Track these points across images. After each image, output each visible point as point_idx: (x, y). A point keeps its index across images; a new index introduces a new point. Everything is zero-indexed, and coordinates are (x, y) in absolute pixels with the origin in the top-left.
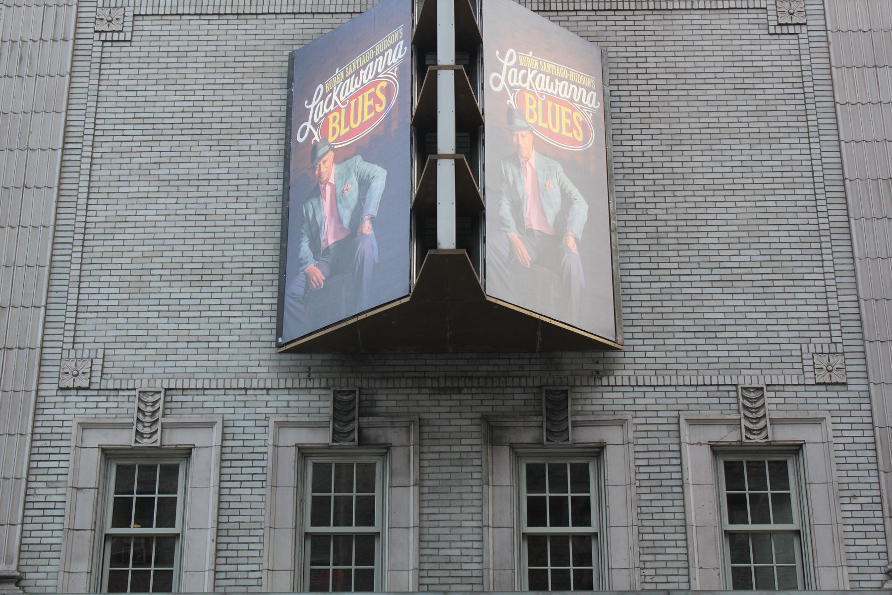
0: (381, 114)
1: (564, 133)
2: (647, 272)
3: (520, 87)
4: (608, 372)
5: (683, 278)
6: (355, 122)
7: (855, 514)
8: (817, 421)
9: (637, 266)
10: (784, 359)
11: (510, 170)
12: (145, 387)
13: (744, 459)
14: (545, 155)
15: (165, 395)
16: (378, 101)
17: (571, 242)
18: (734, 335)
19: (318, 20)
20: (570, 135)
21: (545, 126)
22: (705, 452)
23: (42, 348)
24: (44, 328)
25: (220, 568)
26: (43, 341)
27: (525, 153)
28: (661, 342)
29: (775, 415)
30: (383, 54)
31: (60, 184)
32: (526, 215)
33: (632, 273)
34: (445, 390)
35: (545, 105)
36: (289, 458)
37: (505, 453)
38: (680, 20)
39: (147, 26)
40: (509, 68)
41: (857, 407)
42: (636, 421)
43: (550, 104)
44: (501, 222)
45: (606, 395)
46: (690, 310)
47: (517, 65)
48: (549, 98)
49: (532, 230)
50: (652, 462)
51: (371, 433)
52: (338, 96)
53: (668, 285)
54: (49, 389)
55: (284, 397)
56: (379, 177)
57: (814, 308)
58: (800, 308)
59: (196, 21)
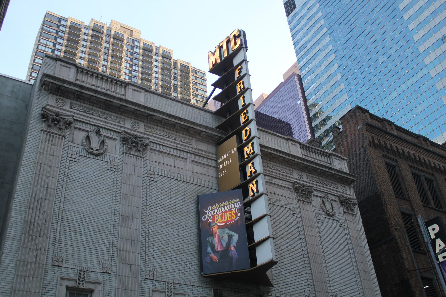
0: (234, 219)
6: (225, 219)
12: (168, 281)
16: (232, 215)
19: (200, 188)
30: (233, 204)
39: (161, 179)
52: (217, 211)
56: (236, 237)
59: (172, 181)
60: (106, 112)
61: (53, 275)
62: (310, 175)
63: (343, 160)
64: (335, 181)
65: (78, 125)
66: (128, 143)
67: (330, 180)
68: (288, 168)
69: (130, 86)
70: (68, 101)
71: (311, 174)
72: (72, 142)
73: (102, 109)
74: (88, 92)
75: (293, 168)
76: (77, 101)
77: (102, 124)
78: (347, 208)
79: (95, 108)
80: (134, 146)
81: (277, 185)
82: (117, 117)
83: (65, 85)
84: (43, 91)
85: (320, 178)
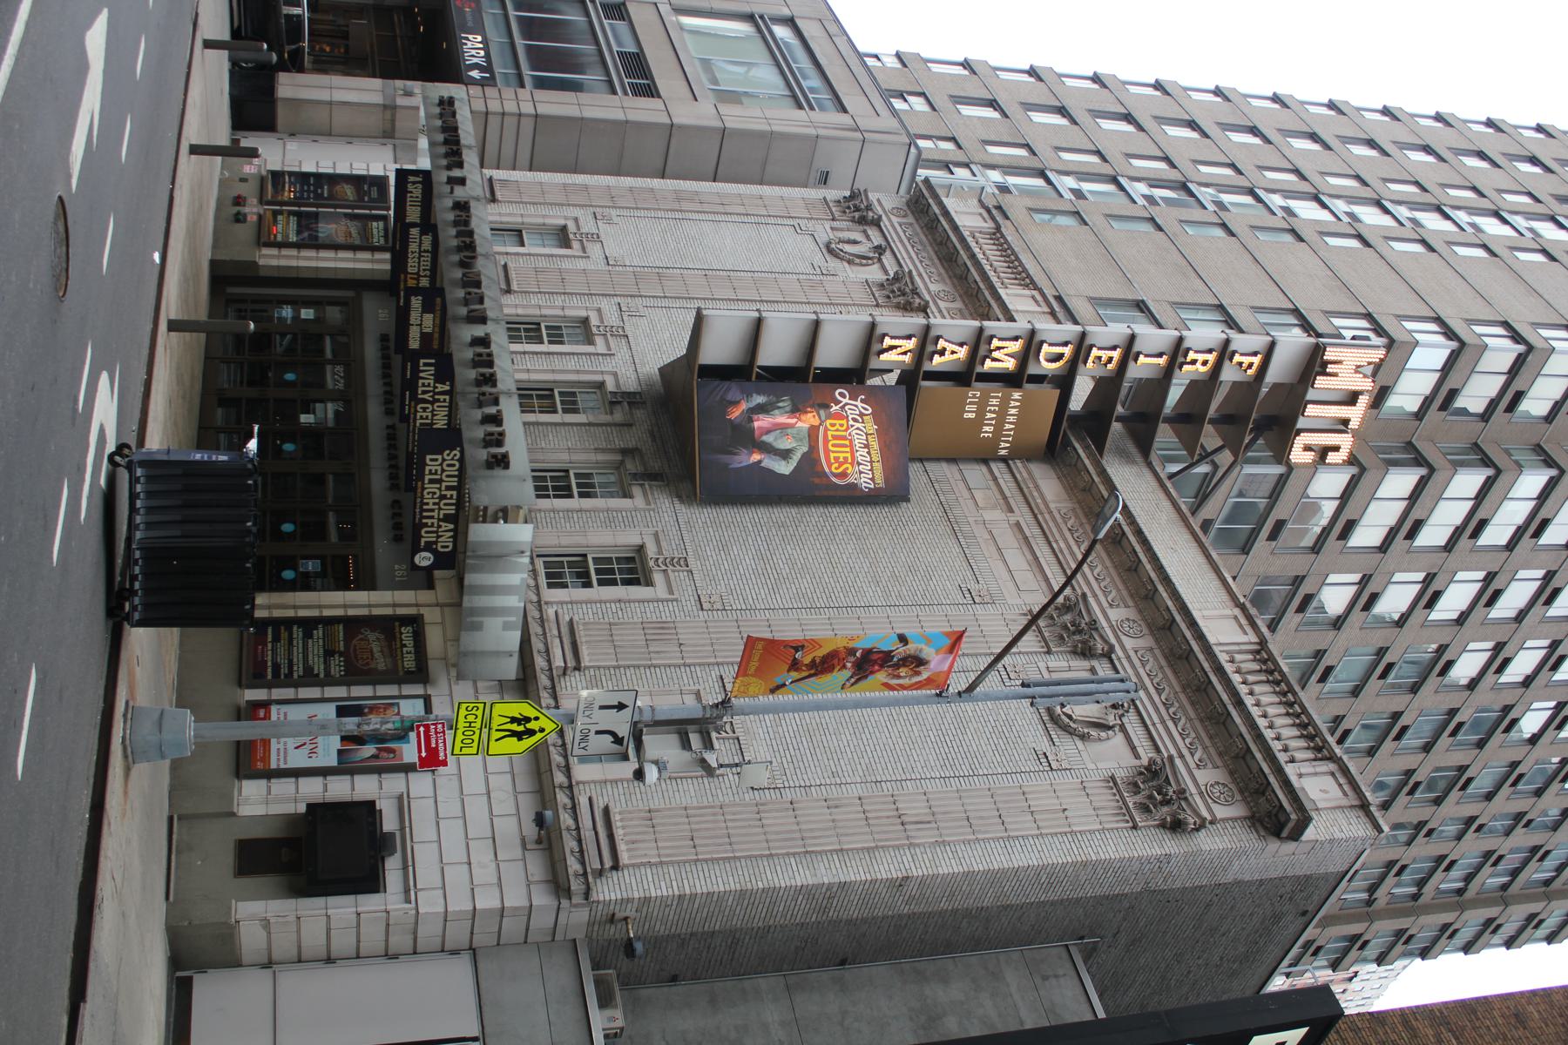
4: (682, 501)
8: (671, 592)
11: (785, 403)
13: (638, 565)
17: (756, 457)
22: (637, 541)
35: (844, 438)
36: (598, 378)
37: (619, 457)
38: (952, 542)
44: (749, 395)
47: (861, 415)
51: (618, 407)
61: (577, 212)
62: (1163, 663)
63: (1364, 819)
64: (1220, 754)
67: (1211, 738)
68: (1125, 593)
69: (1035, 293)
70: (911, 219)
71: (1171, 666)
75: (1137, 606)
78: (1135, 785)
81: (1036, 558)
85: (1182, 697)
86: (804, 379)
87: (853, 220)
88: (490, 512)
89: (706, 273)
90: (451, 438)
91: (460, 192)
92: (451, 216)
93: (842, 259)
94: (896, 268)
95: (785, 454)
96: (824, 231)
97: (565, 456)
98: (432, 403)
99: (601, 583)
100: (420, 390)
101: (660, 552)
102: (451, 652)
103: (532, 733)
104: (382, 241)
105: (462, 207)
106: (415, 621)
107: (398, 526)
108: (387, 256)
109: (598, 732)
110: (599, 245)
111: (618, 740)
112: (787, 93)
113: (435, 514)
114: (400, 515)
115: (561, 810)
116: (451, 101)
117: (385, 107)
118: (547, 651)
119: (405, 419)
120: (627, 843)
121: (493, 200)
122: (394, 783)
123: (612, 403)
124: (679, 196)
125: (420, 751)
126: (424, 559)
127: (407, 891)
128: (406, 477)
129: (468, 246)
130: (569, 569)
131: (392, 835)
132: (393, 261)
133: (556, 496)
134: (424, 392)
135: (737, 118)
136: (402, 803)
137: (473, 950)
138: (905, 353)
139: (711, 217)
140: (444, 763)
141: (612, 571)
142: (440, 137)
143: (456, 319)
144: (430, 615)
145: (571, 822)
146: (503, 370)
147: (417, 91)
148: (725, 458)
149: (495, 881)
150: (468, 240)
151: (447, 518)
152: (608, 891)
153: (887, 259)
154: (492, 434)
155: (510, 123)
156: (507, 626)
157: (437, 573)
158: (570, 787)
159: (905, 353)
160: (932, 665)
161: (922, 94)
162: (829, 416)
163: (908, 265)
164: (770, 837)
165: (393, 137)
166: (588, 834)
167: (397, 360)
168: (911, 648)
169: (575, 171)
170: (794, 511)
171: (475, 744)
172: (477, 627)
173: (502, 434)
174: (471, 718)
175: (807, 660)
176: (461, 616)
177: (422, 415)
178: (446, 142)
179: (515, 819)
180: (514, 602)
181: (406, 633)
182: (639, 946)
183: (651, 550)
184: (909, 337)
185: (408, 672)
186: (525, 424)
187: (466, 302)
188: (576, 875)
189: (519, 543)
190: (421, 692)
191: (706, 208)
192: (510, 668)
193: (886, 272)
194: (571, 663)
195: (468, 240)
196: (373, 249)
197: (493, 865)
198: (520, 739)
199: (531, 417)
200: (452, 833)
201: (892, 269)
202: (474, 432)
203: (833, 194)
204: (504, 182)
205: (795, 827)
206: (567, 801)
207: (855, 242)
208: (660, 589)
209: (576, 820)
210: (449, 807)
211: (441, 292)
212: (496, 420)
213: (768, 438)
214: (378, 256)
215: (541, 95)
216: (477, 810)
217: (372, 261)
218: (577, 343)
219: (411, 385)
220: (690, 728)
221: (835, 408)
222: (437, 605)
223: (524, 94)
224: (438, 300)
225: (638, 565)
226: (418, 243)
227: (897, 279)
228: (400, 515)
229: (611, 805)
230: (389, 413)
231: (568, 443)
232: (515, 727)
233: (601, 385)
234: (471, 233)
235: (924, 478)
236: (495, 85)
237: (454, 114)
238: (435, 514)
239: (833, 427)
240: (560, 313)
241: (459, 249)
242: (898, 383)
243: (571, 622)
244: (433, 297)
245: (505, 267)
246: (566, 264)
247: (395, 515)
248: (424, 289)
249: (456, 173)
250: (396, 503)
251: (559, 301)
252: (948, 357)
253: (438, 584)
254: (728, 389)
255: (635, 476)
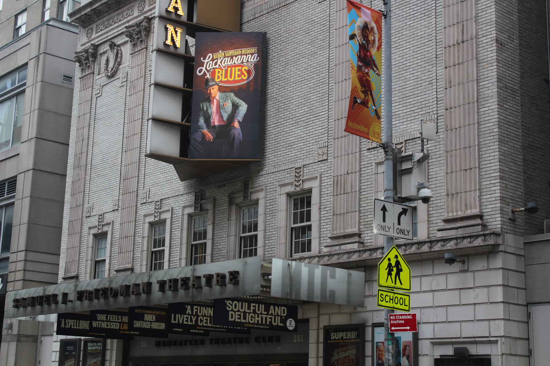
1: (237, 78)
2: (274, 125)
3: (213, 68)
4: (261, 170)
5: (285, 125)
7: (325, 215)
8: (316, 178)
9: (272, 123)
10: (311, 153)
11: (205, 106)
14: (225, 92)
15: (161, 201)
17: (236, 124)
18: (296, 146)
20: (240, 78)
21: (226, 79)
22: (284, 198)
23: (137, 191)
24: (138, 183)
25: (171, 260)
26: (138, 188)
27: (213, 95)
28: (276, 154)
29: (303, 178)
31: (141, 131)
32: (212, 121)
33: (271, 126)
34: (221, 186)
35: (226, 71)
36: (186, 217)
40: (207, 63)
41: (329, 169)
42: (268, 188)
43: (229, 69)
44: (199, 128)
45: (261, 179)
46: (285, 138)
47: (213, 60)
48: (228, 67)
49: (215, 126)
50: (271, 204)
51: (204, 206)
53: (280, 129)
54: (139, 204)
55: (186, 196)
57: (321, 128)
58: (317, 129)
60: (120, 11)
65: (102, 50)
66: (134, 39)
70: (94, 26)
72: (99, 75)
73: (117, 10)
74: (96, 5)
76: (99, 19)
77: (115, 32)
79: (112, 15)
80: (138, 38)
82: (128, 9)
83: (83, 13)
84: (82, 30)
86: (191, 93)
87: (94, 62)
88: (264, 284)
89: (124, 151)
90: (219, 306)
91: (71, 297)
92: (86, 302)
93: (118, 69)
94: (125, 36)
95: (235, 107)
96: (100, 79)
97: (232, 239)
98: (198, 316)
99: (309, 220)
100: (190, 323)
101: (291, 184)
102: (347, 310)
103: (398, 263)
104: (99, 344)
105: (81, 295)
106: (328, 331)
107: (271, 339)
108: (109, 341)
109: (399, 224)
110: (106, 215)
111: (404, 212)
112: (15, 98)
113: (264, 316)
114: (264, 338)
115: (445, 248)
116: (16, 301)
117: (18, 341)
118: (348, 253)
119: (206, 333)
120: (466, 209)
121: (76, 277)
122: (425, 347)
123: (201, 210)
124: (77, 166)
125: (406, 330)
126: (291, 324)
127: (490, 342)
128: (242, 333)
129: (104, 293)
130: (300, 240)
131: (456, 350)
132: (112, 338)
133: (256, 245)
134: (191, 321)
135: (30, 130)
136: (437, 343)
137: (528, 305)
138: (176, 32)
139: (90, 147)
140: (414, 316)
141: (302, 213)
142: (38, 307)
143: (148, 300)
144: (325, 321)
145: (452, 243)
146: (180, 272)
147: (9, 322)
148: (236, 143)
149: (486, 289)
150: (101, 292)
151: (267, 310)
152: (495, 222)
153: (118, 41)
154: (218, 281)
155: (30, 266)
156: (333, 276)
157: (300, 317)
158: (431, 242)
159: (176, 32)
160: (367, 20)
161: (16, 16)
162: (213, 79)
163: (122, 29)
164: (467, 123)
165: (37, 336)
166: (460, 233)
167: (171, 337)
168: (357, 32)
169: (61, 228)
170: (270, 103)
171: (403, 297)
172: (333, 293)
173: (218, 275)
174: (388, 299)
175: (362, 96)
176: (325, 303)
177: (205, 322)
178: (41, 304)
179: (449, 276)
180: (318, 271)
181: (334, 336)
182: (530, 205)
183: (290, 189)
184: (166, 29)
185: (358, 336)
186: (212, 261)
187: (138, 294)
188: (485, 240)
189: (283, 267)
190: (370, 329)
191: (85, 150)
192: (358, 275)
193: (126, 42)
194: (356, 239)
195: (101, 292)
196: (104, 349)
197: (477, 290)
198: (401, 270)
199: (208, 258)
200: (456, 314)
201: (125, 39)
202: (216, 291)
203: (78, 73)
204: (66, 270)
205: (462, 108)
206: (439, 245)
207: (107, 61)
208: (314, 185)
209: (451, 239)
210: (441, 314)
211: (132, 309)
212: (209, 278)
213: (225, 117)
214: (109, 347)
215: (14, 247)
216: (443, 298)
217: (112, 350)
218: (164, 230)
219: (186, 328)
220: (398, 168)
221: (208, 76)
222: (318, 317)
223: (13, 257)
224: (137, 311)
225: (299, 197)
226: (101, 322)
227: (130, 36)
228: (264, 338)
229: (443, 218)
230: (202, 342)
231: (224, 236)
232: (394, 273)
233: (190, 216)
234: (97, 290)
235: (252, 23)
236: (7, 274)
237: (24, 299)
238: (264, 316)
239: (220, 77)
240: (146, 239)
241: (106, 298)
242: (193, 36)
243: (330, 238)
244: (135, 314)
245: (117, 271)
246: (117, 235)
247: (264, 341)
248: (129, 319)
249: (60, 298)
250: (257, 340)
251: (139, 240)
252: (179, 6)
253: (307, 316)
254: (195, 140)
255: (245, 197)
